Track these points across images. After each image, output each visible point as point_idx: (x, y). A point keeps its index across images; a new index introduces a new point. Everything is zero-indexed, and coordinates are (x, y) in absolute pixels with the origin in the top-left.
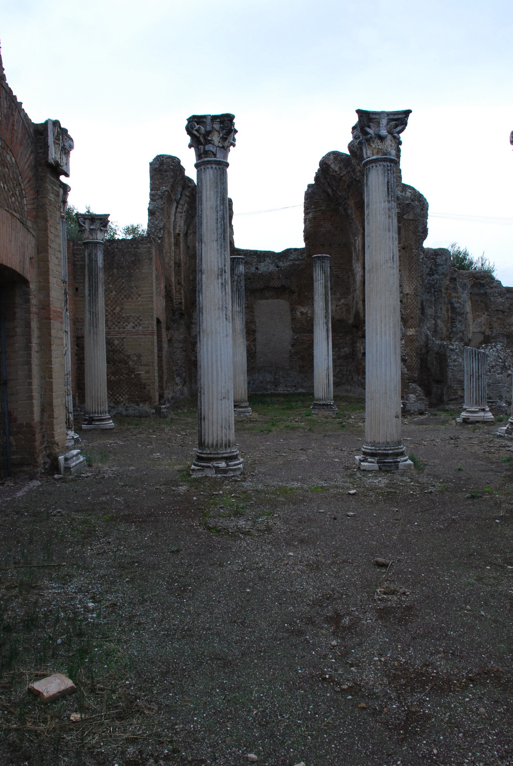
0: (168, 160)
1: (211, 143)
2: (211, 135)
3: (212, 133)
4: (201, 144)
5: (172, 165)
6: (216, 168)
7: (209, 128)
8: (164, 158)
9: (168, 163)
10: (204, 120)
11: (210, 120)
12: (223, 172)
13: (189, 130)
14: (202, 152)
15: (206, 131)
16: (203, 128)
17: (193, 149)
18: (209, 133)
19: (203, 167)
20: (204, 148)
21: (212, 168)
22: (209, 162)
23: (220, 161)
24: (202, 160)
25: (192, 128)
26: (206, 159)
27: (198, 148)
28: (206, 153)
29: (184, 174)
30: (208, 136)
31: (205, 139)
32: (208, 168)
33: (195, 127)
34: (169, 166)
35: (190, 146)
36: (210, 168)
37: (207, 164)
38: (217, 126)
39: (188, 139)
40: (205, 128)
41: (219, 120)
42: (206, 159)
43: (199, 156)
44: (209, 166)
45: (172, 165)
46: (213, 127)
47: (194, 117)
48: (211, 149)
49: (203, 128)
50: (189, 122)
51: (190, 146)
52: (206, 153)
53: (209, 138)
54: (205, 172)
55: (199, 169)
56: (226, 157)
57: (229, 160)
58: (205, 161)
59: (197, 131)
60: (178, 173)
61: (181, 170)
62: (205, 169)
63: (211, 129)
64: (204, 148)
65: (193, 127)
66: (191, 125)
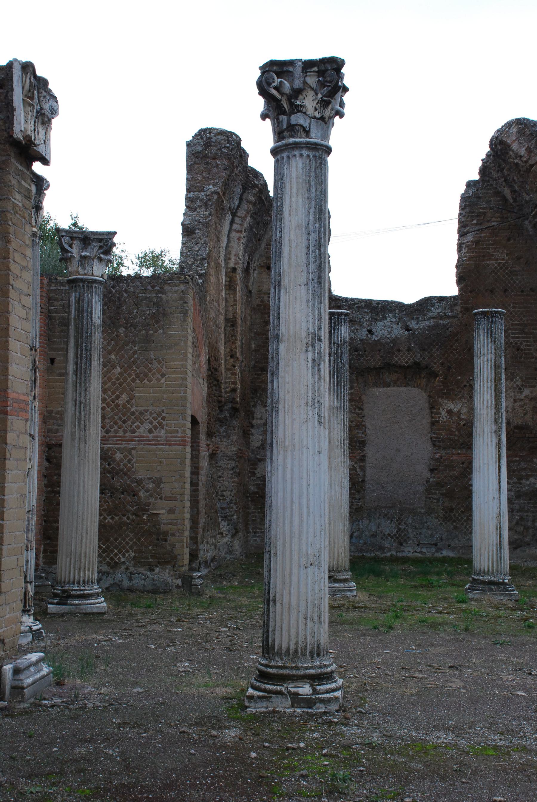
0: (220, 138)
1: (301, 111)
2: (301, 97)
3: (304, 94)
4: (284, 113)
5: (225, 147)
6: (308, 156)
7: (298, 84)
8: (212, 135)
9: (220, 143)
10: (291, 69)
11: (300, 69)
12: (321, 164)
13: (263, 87)
14: (285, 127)
15: (293, 89)
16: (287, 84)
17: (268, 121)
18: (297, 93)
19: (285, 155)
20: (289, 120)
21: (301, 155)
22: (296, 146)
23: (316, 144)
24: (284, 142)
25: (269, 84)
26: (291, 140)
27: (278, 119)
28: (292, 129)
29: (247, 163)
30: (296, 98)
31: (291, 104)
32: (295, 156)
33: (274, 82)
34: (220, 149)
35: (264, 117)
36: (298, 155)
37: (293, 148)
38: (312, 80)
39: (260, 103)
40: (292, 83)
41: (316, 69)
42: (291, 140)
43: (279, 134)
44: (296, 152)
45: (225, 147)
46: (305, 83)
47: (272, 63)
48: (301, 122)
49: (287, 84)
50: (263, 73)
51: (264, 117)
52: (292, 129)
53: (298, 103)
54: (289, 163)
55: (279, 157)
56: (326, 136)
57: (332, 142)
58: (290, 144)
59: (276, 88)
60: (236, 161)
61: (241, 156)
62: (288, 157)
63: (301, 86)
64: (289, 120)
65: (271, 81)
66: (266, 79)
